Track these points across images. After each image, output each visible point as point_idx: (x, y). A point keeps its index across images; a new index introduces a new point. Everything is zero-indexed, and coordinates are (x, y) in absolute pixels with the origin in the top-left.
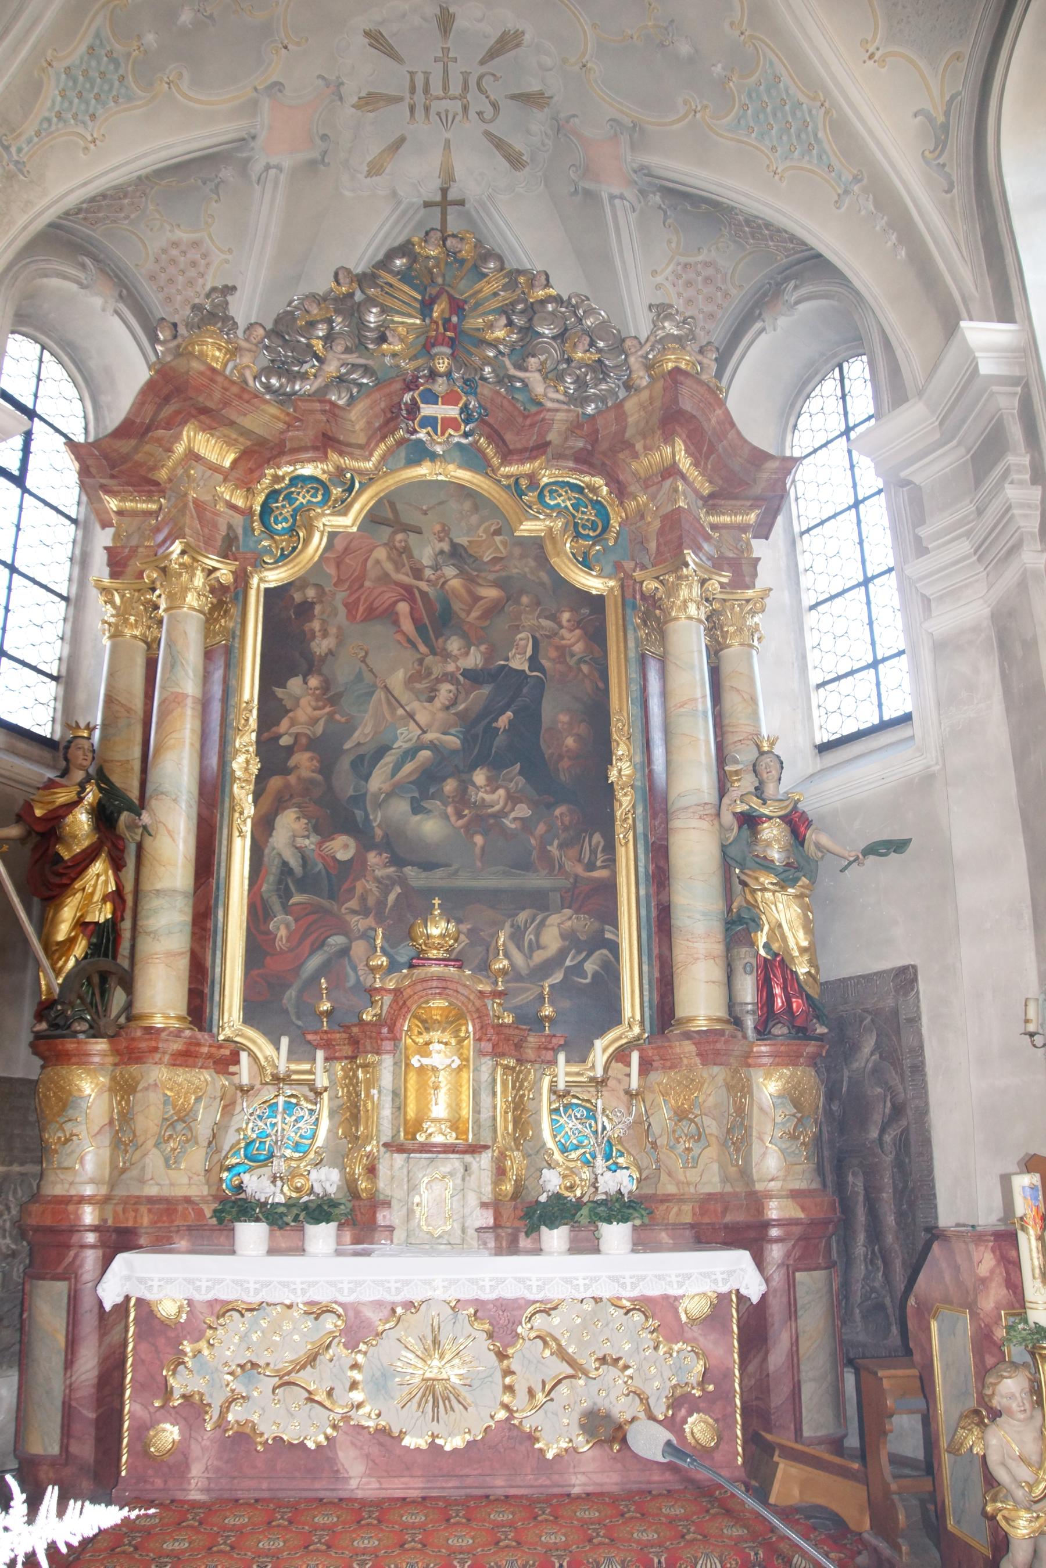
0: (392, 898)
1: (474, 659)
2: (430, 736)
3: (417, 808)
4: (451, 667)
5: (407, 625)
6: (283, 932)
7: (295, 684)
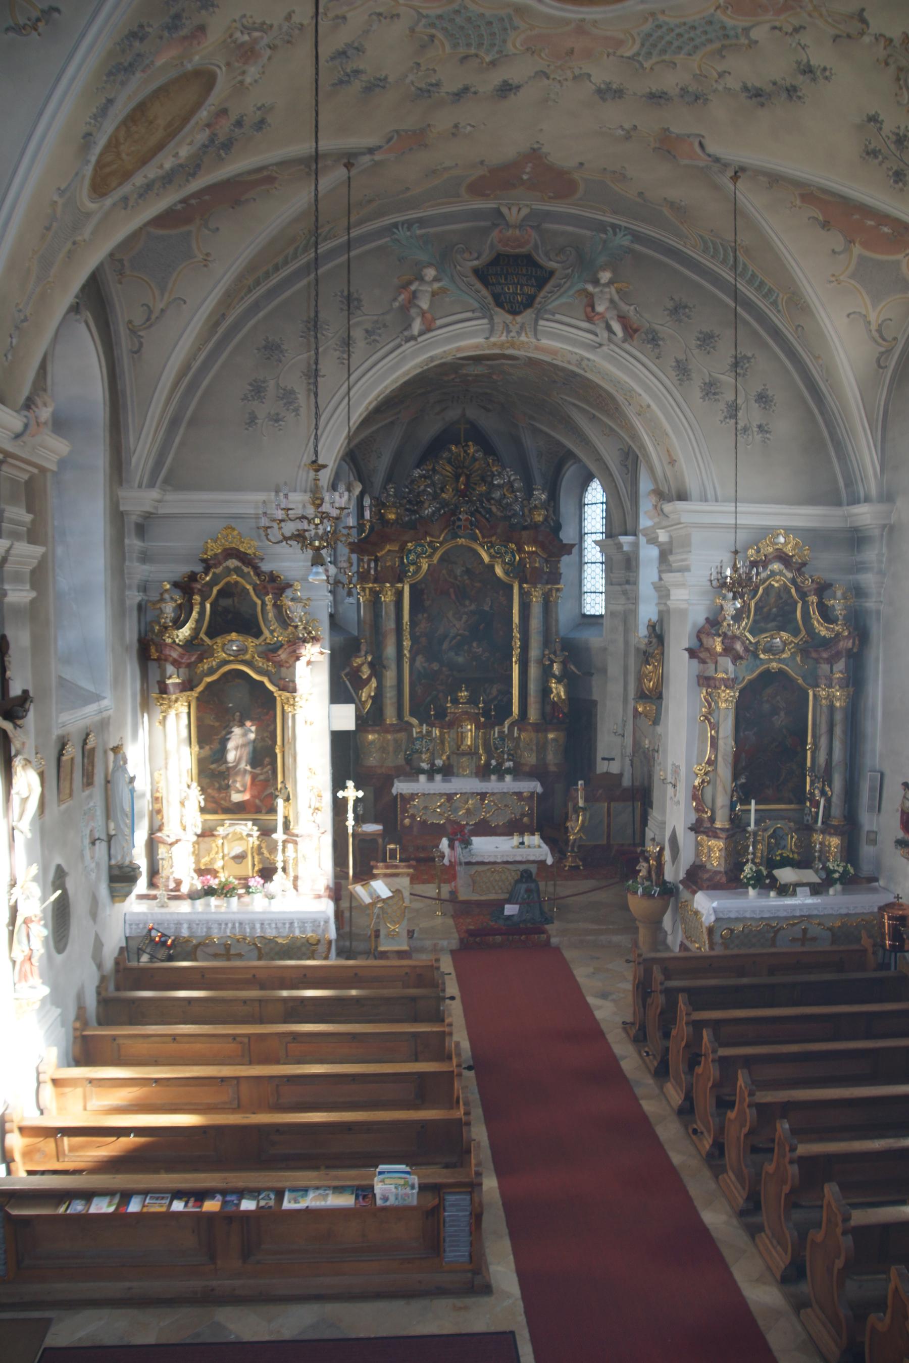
0: (450, 680)
1: (473, 607)
2: (460, 632)
3: (457, 654)
4: (466, 610)
5: (453, 596)
6: (419, 691)
7: (420, 616)
